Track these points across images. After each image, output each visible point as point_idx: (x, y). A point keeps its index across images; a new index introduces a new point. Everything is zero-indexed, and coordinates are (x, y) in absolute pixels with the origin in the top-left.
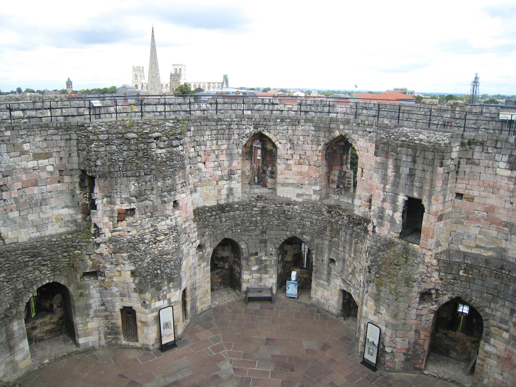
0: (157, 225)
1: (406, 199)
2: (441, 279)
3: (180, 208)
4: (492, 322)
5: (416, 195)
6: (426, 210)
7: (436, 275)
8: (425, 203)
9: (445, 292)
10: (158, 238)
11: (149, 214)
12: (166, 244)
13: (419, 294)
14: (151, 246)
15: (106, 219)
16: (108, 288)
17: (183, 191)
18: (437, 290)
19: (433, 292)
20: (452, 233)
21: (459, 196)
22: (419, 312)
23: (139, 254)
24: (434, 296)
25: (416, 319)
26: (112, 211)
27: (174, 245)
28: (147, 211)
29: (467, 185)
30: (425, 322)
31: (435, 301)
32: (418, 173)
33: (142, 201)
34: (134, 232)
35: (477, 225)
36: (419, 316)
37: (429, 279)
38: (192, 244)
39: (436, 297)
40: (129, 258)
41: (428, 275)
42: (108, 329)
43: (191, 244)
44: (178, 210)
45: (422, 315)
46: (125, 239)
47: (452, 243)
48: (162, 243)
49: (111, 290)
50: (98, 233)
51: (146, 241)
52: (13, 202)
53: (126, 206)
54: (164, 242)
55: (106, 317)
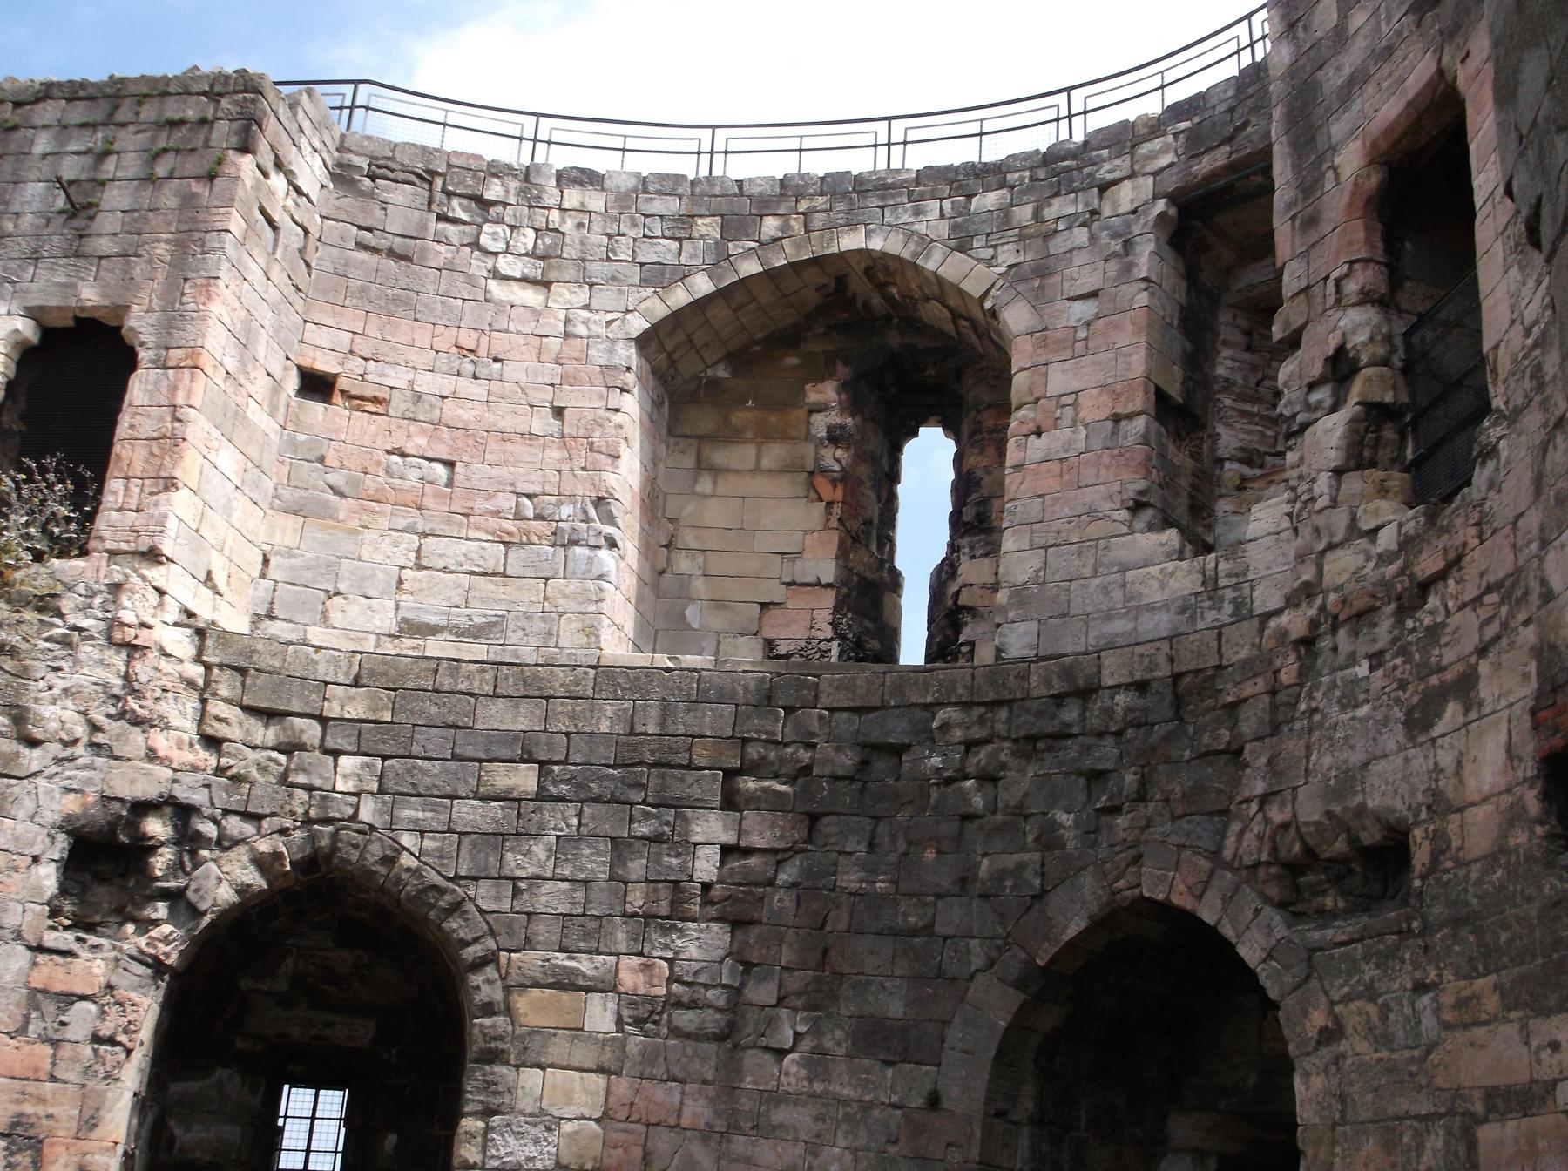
1: (27, 328)
2: (213, 743)
4: (530, 960)
5: (90, 295)
6: (144, 355)
7: (181, 713)
8: (141, 324)
9: (234, 825)
13: (63, 841)
18: (183, 812)
19: (156, 827)
20: (273, 561)
21: (316, 385)
22: (51, 973)
24: (161, 861)
25: (23, 1030)
29: (358, 339)
30: (87, 1051)
31: (165, 895)
32: (116, 198)
35: (401, 523)
36: (50, 1007)
37: (136, 735)
39: (178, 867)
41: (133, 703)
45: (68, 999)
47: (271, 617)
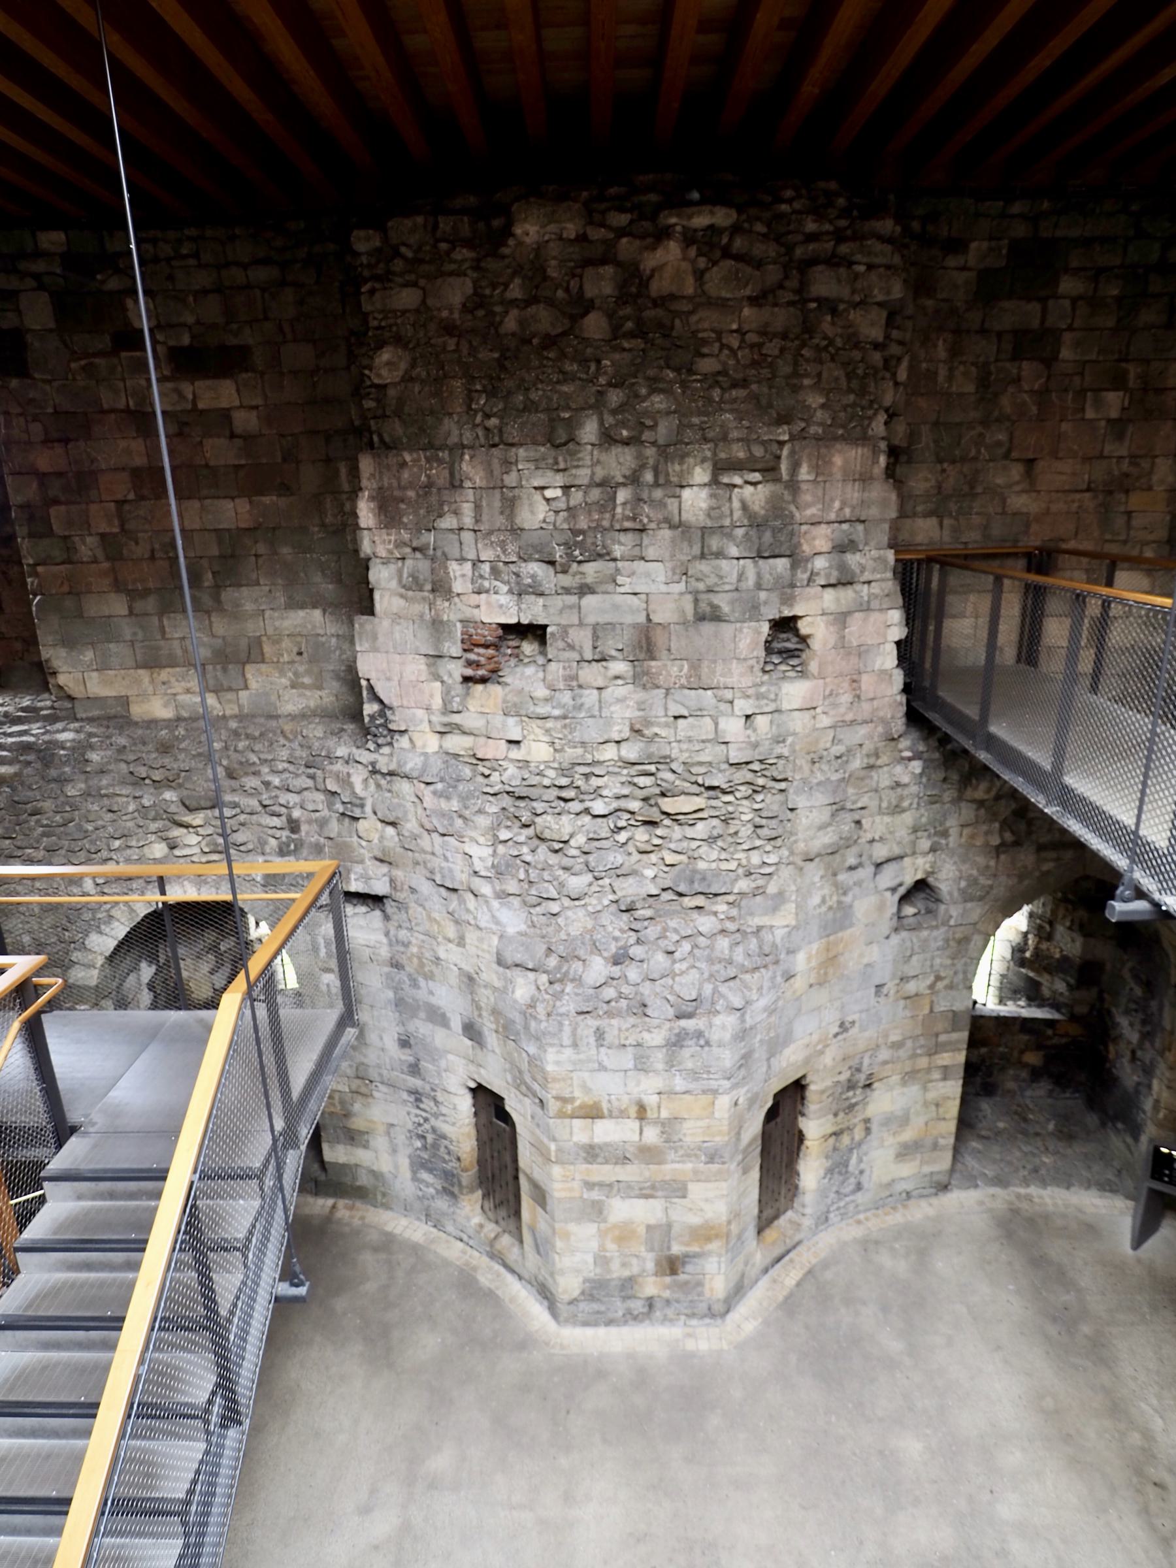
0: (663, 732)
3: (813, 667)
10: (668, 805)
11: (620, 667)
12: (711, 840)
14: (622, 837)
15: (416, 668)
16: (422, 982)
17: (843, 567)
23: (553, 859)
26: (437, 626)
27: (755, 858)
28: (610, 646)
33: (585, 590)
34: (538, 750)
38: (878, 865)
40: (499, 872)
42: (425, 1147)
43: (867, 871)
44: (803, 674)
46: (495, 777)
48: (690, 832)
49: (431, 993)
50: (385, 726)
51: (599, 807)
52: (100, 554)
53: (500, 608)
54: (701, 830)
55: (417, 1096)
